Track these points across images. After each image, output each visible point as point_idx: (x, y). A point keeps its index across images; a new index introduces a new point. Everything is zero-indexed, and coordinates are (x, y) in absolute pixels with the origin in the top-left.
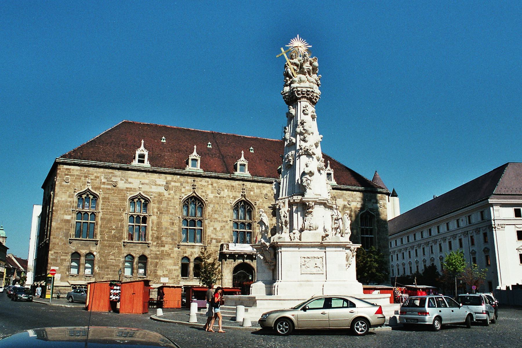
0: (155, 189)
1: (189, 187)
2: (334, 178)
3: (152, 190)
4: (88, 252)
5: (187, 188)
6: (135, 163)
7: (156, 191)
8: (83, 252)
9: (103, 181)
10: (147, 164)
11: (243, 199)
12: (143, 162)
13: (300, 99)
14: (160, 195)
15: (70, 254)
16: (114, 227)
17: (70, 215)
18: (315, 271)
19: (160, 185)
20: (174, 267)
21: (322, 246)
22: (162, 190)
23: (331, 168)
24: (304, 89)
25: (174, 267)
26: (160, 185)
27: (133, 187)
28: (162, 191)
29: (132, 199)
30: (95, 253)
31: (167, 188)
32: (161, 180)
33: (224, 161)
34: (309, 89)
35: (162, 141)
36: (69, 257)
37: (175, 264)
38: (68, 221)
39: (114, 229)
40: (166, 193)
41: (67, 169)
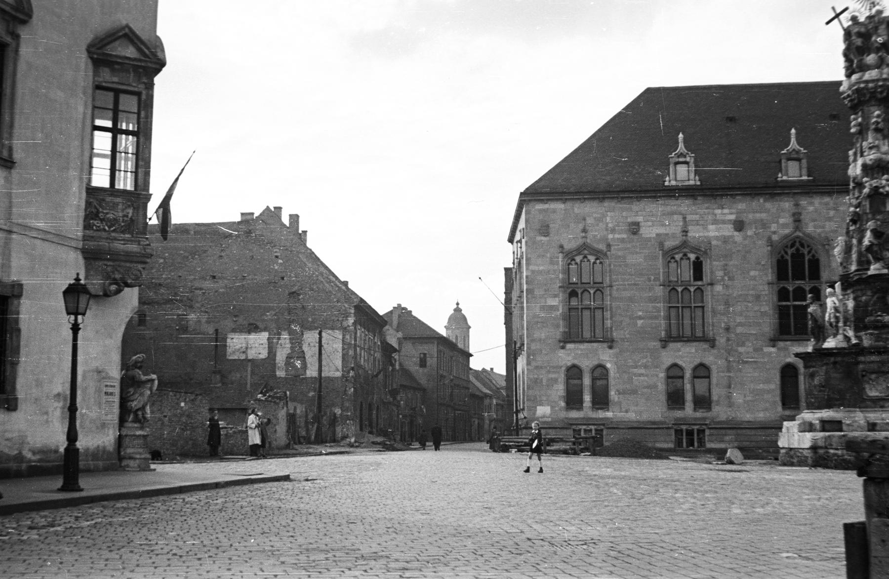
0: (713, 232)
1: (786, 219)
3: (712, 234)
4: (596, 363)
5: (781, 221)
7: (717, 234)
8: (586, 364)
14: (725, 240)
15: (564, 369)
17: (555, 296)
19: (724, 222)
20: (766, 387)
22: (728, 230)
25: (766, 387)
26: (724, 222)
27: (670, 232)
28: (730, 234)
30: (608, 365)
31: (739, 226)
32: (727, 212)
36: (562, 377)
37: (768, 381)
38: (552, 308)
39: (640, 318)
40: (738, 236)
41: (541, 211)
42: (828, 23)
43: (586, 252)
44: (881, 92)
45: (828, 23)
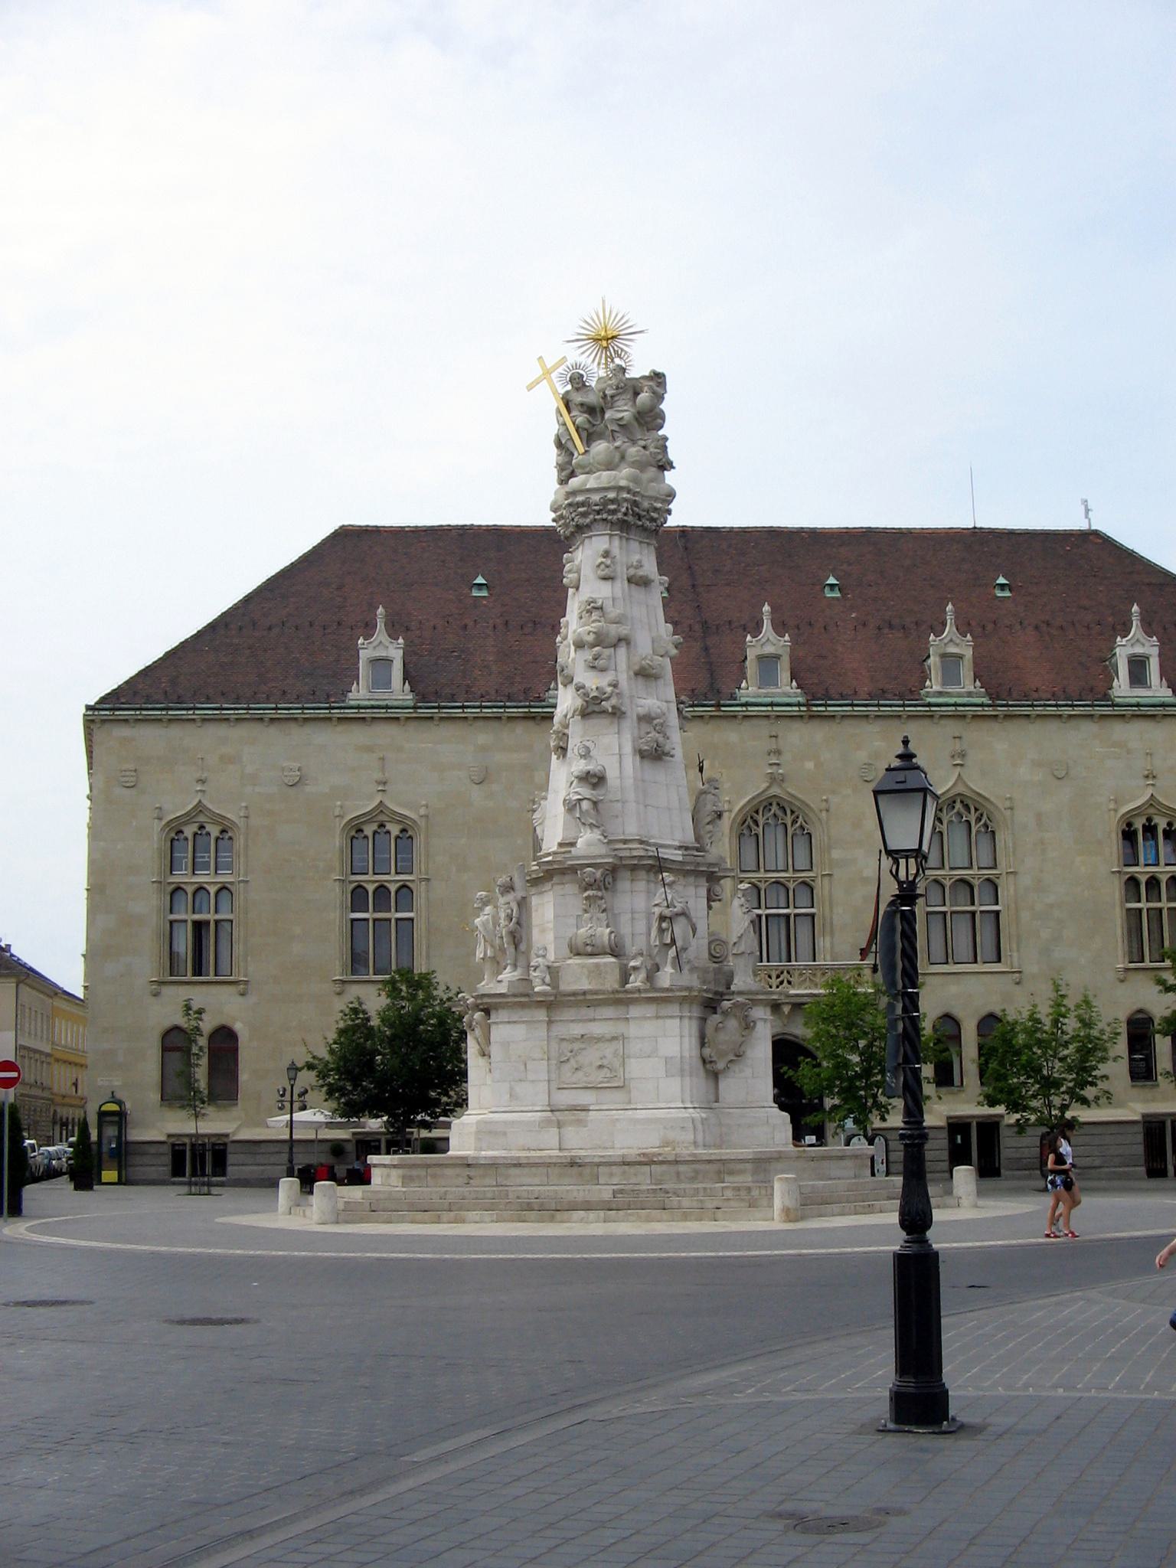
2: (1163, 674)
6: (360, 693)
9: (249, 769)
10: (399, 691)
11: (775, 790)
12: (388, 684)
13: (588, 527)
16: (297, 930)
18: (598, 1077)
21: (618, 1002)
23: (1148, 628)
24: (596, 498)
29: (355, 830)
33: (706, 649)
34: (611, 495)
35: (475, 593)
42: (530, 388)
43: (201, 818)
44: (614, 512)
45: (530, 388)
